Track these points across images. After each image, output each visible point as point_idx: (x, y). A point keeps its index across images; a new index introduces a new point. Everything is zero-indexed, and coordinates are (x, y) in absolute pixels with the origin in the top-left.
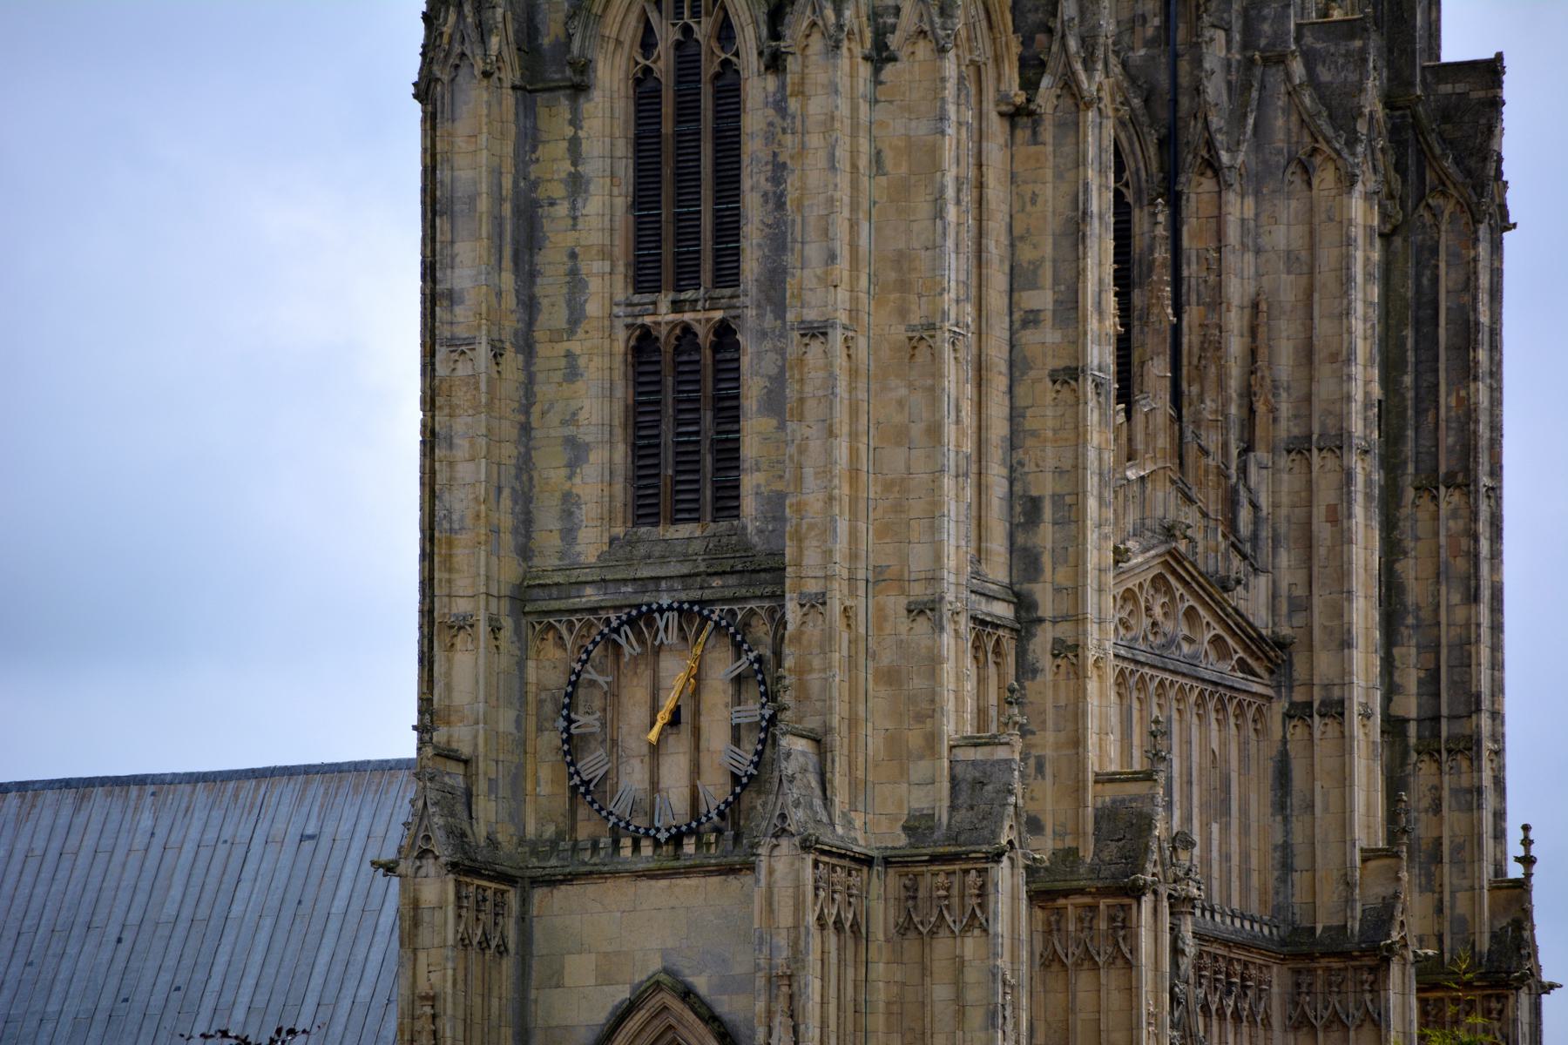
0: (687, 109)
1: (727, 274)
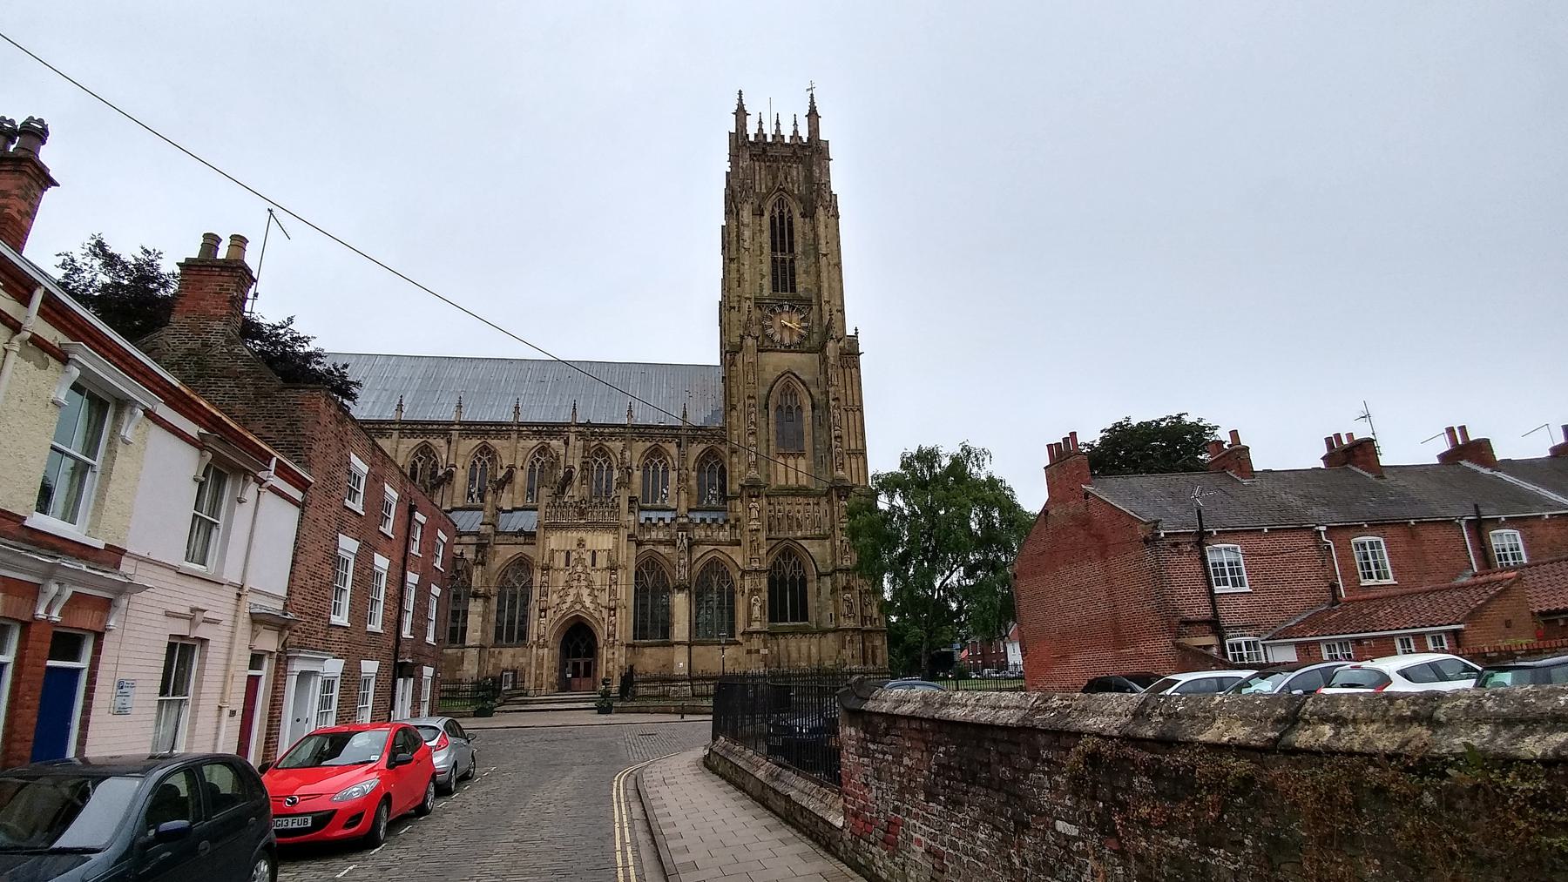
0: (782, 223)
1: (791, 250)
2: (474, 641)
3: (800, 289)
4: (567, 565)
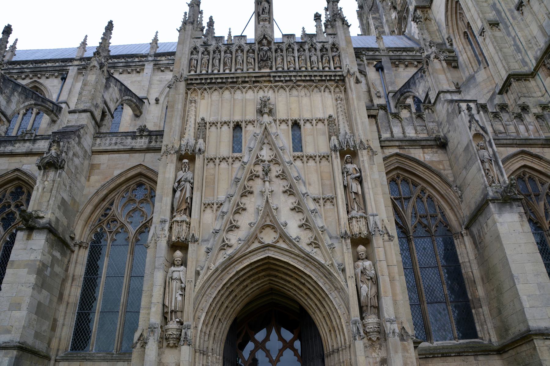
2: (8, 331)
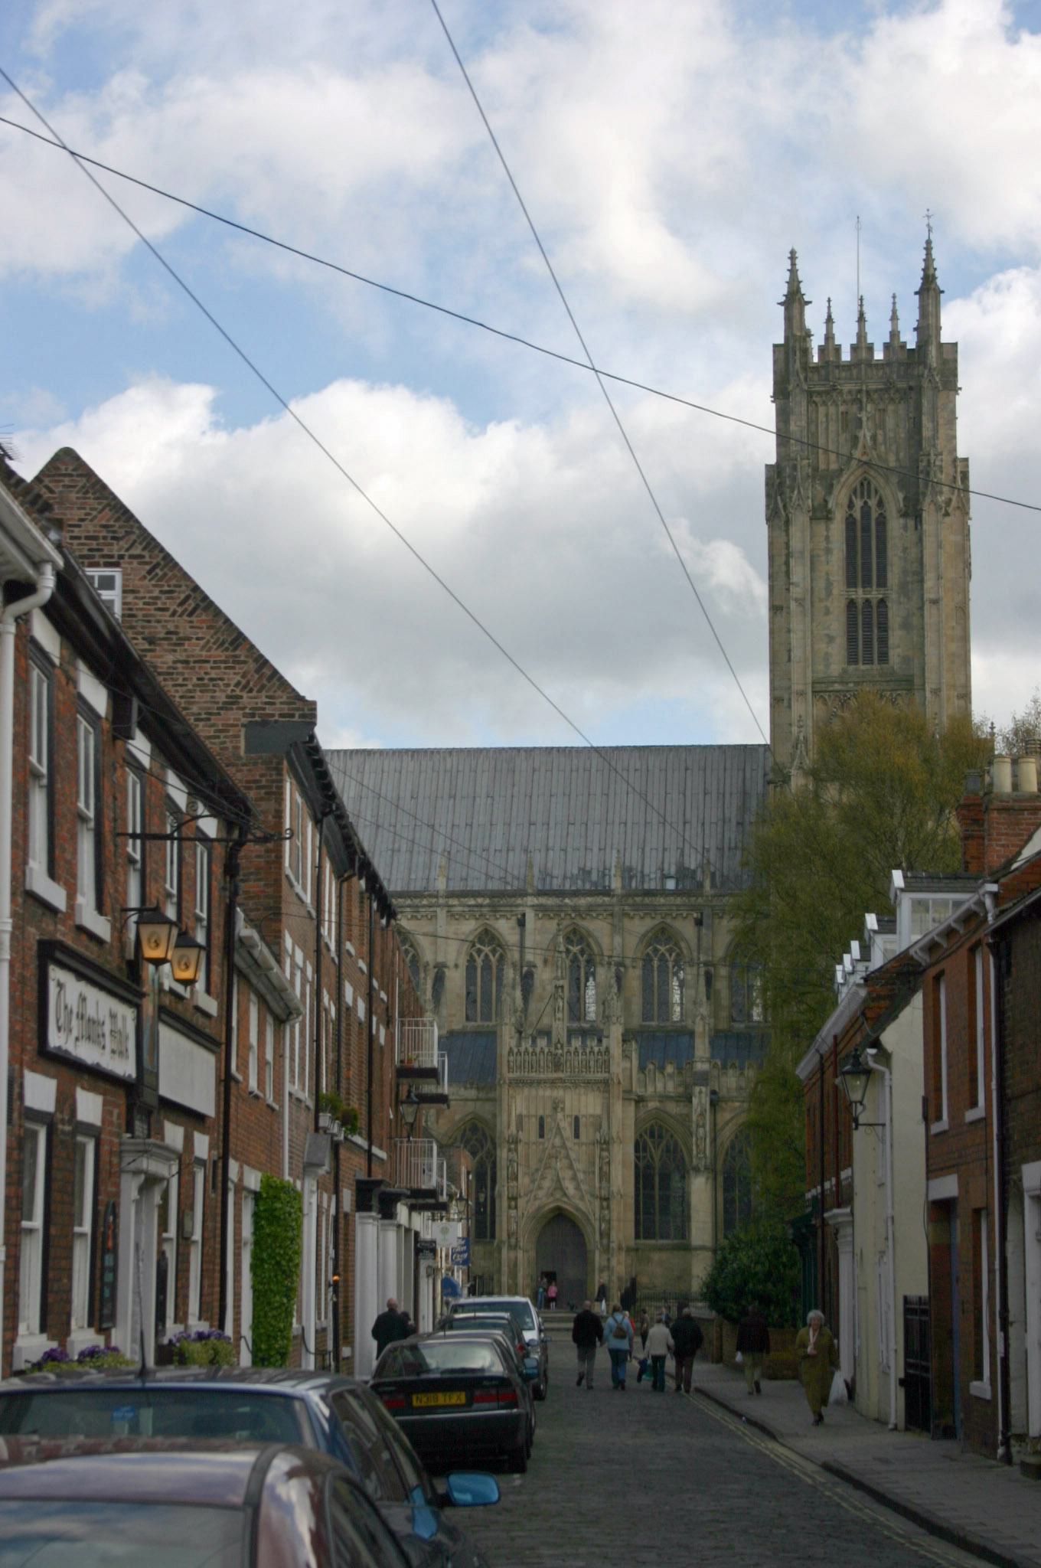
1: (882, 582)
3: (895, 655)
4: (542, 1136)
